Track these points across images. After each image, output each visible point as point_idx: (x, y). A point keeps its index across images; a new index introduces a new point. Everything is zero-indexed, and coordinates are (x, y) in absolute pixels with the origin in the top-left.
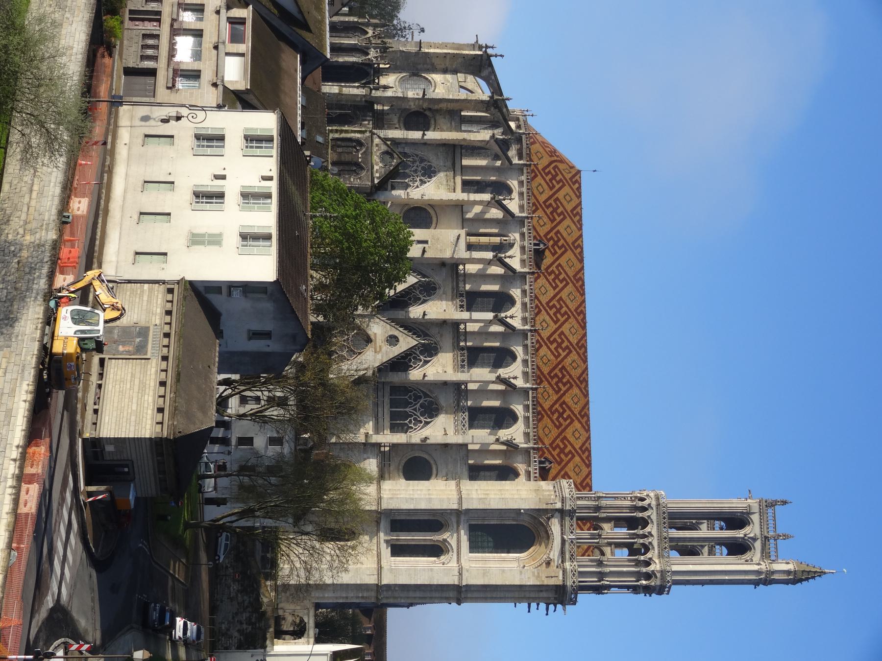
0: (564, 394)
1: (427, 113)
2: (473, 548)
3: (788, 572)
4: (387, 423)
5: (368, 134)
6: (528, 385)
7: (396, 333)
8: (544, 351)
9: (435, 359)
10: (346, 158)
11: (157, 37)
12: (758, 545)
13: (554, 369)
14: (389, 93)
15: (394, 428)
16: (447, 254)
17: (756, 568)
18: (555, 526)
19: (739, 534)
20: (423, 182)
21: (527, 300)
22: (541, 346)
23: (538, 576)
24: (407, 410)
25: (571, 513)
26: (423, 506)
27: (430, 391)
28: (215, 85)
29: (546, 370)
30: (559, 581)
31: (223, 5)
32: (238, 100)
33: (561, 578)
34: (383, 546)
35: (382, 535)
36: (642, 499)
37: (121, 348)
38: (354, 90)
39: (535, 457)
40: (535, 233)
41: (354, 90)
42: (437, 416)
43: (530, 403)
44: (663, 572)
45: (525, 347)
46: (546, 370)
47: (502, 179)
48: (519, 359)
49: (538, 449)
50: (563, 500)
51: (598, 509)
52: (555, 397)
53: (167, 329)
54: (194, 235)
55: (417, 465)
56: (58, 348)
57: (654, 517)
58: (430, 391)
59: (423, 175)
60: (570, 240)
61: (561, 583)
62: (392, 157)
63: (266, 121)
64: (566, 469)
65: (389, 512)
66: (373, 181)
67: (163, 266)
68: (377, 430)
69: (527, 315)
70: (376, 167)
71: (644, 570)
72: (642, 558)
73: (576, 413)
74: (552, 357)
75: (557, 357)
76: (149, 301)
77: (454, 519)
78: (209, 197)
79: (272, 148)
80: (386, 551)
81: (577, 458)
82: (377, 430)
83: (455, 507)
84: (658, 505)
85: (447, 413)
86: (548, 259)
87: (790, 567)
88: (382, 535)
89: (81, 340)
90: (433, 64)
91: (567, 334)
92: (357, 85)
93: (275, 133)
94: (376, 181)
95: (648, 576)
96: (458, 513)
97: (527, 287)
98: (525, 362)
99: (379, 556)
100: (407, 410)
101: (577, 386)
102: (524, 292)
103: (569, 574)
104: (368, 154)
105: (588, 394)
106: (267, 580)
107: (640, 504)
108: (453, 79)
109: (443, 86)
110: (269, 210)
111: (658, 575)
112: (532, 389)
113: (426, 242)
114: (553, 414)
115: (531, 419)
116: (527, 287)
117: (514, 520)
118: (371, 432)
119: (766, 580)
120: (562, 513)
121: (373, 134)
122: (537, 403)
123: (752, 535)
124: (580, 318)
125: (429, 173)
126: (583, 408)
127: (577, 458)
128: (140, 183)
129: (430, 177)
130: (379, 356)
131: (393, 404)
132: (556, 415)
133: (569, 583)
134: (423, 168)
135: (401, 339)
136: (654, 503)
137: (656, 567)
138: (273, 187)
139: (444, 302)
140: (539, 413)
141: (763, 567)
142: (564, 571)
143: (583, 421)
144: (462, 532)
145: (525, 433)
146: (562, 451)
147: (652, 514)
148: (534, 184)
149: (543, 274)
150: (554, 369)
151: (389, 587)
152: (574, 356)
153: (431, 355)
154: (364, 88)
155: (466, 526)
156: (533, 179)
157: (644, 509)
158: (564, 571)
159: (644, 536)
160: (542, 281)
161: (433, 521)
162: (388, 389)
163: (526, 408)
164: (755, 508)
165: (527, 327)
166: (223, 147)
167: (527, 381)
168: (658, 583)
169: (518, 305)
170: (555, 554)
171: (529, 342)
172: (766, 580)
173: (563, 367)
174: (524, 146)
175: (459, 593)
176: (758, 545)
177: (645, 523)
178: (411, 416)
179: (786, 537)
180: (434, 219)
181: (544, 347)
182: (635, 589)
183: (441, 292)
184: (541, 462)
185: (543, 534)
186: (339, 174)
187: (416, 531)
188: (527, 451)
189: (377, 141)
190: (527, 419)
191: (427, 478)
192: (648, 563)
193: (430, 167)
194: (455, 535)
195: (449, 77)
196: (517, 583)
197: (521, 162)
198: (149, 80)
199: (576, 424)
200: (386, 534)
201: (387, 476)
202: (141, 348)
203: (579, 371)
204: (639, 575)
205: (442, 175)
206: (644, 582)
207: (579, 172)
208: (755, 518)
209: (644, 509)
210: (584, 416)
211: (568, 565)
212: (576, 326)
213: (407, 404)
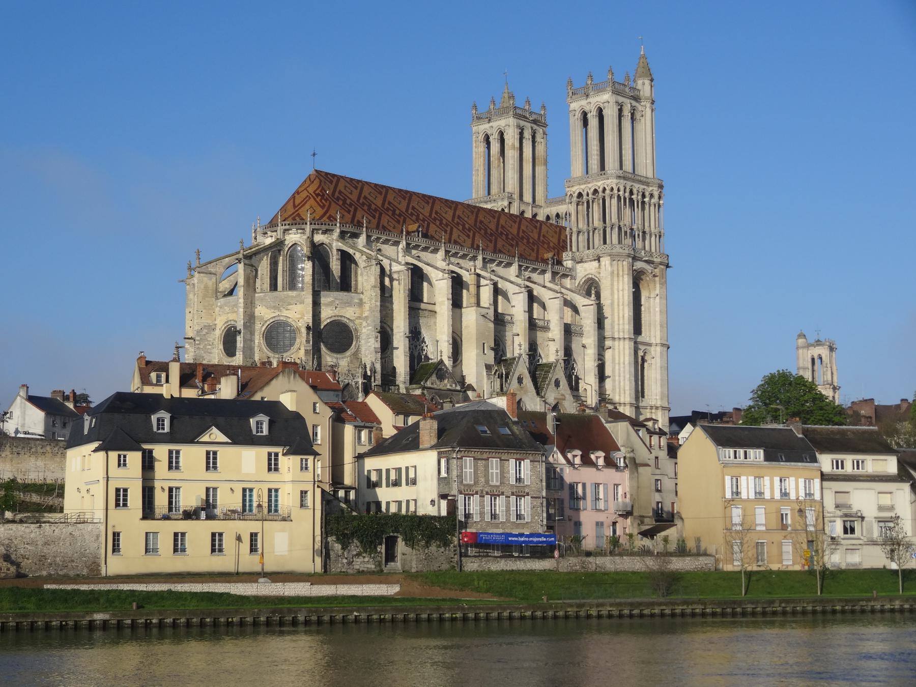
7: (553, 380)
20: (423, 341)
36: (619, 190)
48: (495, 268)
59: (418, 340)
70: (449, 387)
87: (647, 82)
108: (326, 296)
129: (420, 333)
130: (567, 396)
136: (622, 181)
139: (507, 333)
141: (648, 105)
145: (539, 274)
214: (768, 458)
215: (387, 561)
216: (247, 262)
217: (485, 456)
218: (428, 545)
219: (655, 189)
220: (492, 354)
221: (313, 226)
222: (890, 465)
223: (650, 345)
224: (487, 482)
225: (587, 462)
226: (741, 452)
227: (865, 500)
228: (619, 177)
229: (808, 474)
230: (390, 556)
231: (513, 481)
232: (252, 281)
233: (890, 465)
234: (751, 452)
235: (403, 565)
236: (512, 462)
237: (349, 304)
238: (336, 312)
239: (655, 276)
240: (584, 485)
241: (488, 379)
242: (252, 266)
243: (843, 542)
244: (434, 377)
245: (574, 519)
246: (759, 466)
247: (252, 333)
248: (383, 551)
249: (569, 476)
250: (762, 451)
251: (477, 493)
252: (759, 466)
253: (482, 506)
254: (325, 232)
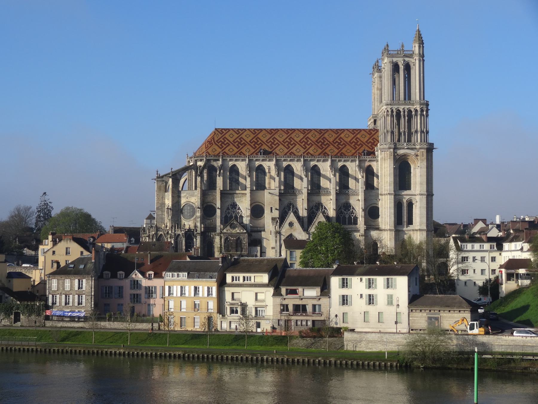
0: (329, 141)
1: (204, 206)
2: (409, 189)
3: (419, 47)
4: (354, 226)
5: (222, 235)
8: (310, 151)
9: (324, 204)
10: (234, 245)
11: (297, 321)
12: (407, 59)
13: (318, 146)
14: (198, 224)
15: (356, 223)
16: (277, 198)
17: (417, 62)
18: (401, 152)
19: (402, 68)
20: (239, 209)
21: (289, 159)
22: (309, 153)
23: (422, 160)
24: (347, 217)
25: (395, 145)
26: (393, 211)
28: (319, 299)
29: (320, 151)
30: (425, 151)
31: (281, 297)
32: (325, 290)
34: (409, 228)
35: (404, 229)
37: (437, 325)
38: (198, 242)
39: (363, 158)
40: (254, 154)
41: (198, 242)
42: (350, 204)
43: (337, 159)
44: (421, 104)
45: (311, 160)
46: (320, 151)
47: (228, 169)
48: (317, 164)
49: (359, 156)
50: (390, 148)
51: (392, 133)
53: (428, 311)
54: (388, 304)
55: (372, 213)
56: (483, 333)
57: (396, 107)
59: (236, 208)
60: (253, 136)
62: (233, 223)
63: (335, 281)
64: (364, 142)
65: (395, 227)
66: (245, 233)
67: (402, 313)
68: (358, 231)
69: (296, 159)
70: (238, 231)
71: (419, 113)
72: (413, 113)
73: (336, 136)
74: (313, 147)
75: (312, 145)
76: (417, 317)
77: (397, 197)
78: (371, 300)
79: (347, 279)
80: (411, 227)
81: (358, 136)
82: (358, 231)
83: (393, 196)
84: (391, 105)
85: (349, 199)
86: (264, 147)
87: (417, 45)
88: (404, 229)
89: (480, 327)
90: (176, 202)
92: (195, 240)
93: (341, 277)
94: (245, 231)
95: (422, 111)
96: (395, 195)
97: (283, 159)
98: (318, 161)
99: (413, 230)
100: (347, 217)
101: (323, 134)
102: (284, 160)
103: (422, 146)
104: (232, 235)
105: (327, 129)
106: (425, 280)
107: (390, 113)
108: (184, 193)
109: (192, 198)
110: (376, 279)
111: (422, 106)
112: (331, 158)
113: (271, 208)
114: (340, 148)
116: (283, 159)
118: (359, 234)
119: (422, 56)
120: (395, 149)
121: (221, 233)
122: (336, 156)
123: (402, 62)
124: (291, 132)
125: (234, 206)
126: (334, 132)
127: (358, 136)
128: (365, 323)
129: (236, 205)
132: (340, 146)
133: (426, 147)
134: (232, 208)
135: (319, 220)
136: (390, 107)
137: (418, 107)
138: (365, 278)
140: (341, 155)
141: (417, 58)
142: (420, 148)
143: (340, 132)
144: (403, 193)
147: (395, 108)
148: (230, 154)
149: (273, 150)
150: (318, 146)
151: (427, 226)
152: (309, 136)
153: (322, 206)
154: (196, 237)
155: (400, 191)
156: (227, 154)
157: (392, 111)
158: (420, 148)
159: (404, 112)
160: (277, 151)
161: (398, 206)
163: (340, 161)
164: (390, 59)
165: (302, 160)
166: (347, 296)
167: (327, 160)
168: (425, 106)
169: (291, 163)
170: (412, 152)
171: (309, 159)
172: (422, 56)
173: (316, 141)
174: (212, 158)
175: (429, 195)
176: (407, 59)
177: (398, 112)
179: (403, 46)
180: (257, 203)
181: (309, 151)
182: (427, 116)
184: (364, 155)
185: (403, 157)
186: (242, 249)
187: (402, 214)
188: (360, 161)
189: (225, 231)
190: (345, 161)
191: (377, 209)
192: (416, 111)
193: (231, 205)
194: (405, 197)
195: (182, 195)
196: (425, 170)
197: (221, 160)
198: (316, 323)
199: (342, 136)
200: (404, 227)
201: (377, 227)
202: (437, 319)
203: (316, 133)
204: (422, 115)
205: (235, 200)
206: (425, 113)
207: (216, 129)
208: (395, 60)
209: (392, 111)
210: (338, 132)
211: (418, 147)
213: (344, 218)
214: (189, 277)
215: (15, 322)
216: (159, 179)
217: (63, 278)
218: (30, 316)
219: (418, 106)
220: (277, 212)
221: (195, 159)
222: (264, 278)
223: (415, 195)
224: (64, 289)
225: (158, 275)
226: (176, 274)
227: (246, 296)
228: (387, 105)
229: (209, 285)
230: (17, 319)
231: (76, 288)
232: (163, 188)
233: (264, 278)
234: (181, 274)
235: (22, 323)
236: (77, 281)
237: (193, 195)
238: (187, 200)
239: (417, 156)
240: (155, 287)
241: (273, 225)
242: (163, 181)
243: (228, 318)
244: (228, 227)
245: (148, 303)
246: (183, 281)
247: (163, 211)
248: (13, 318)
249: (145, 283)
250: (186, 273)
251: (58, 294)
252: (183, 281)
253: (60, 299)
254: (201, 160)
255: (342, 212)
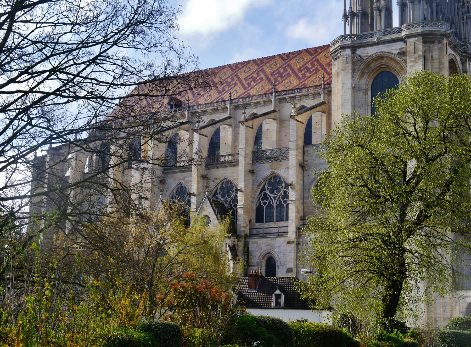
6: (273, 100)
24: (275, 205)
27: (259, 186)
33: (416, 39)
52: (293, 77)
58: (259, 186)
61: (421, 38)
74: (260, 84)
91: (248, 74)
100: (275, 205)
115: (301, 94)
117: (366, 93)
131: (270, 220)
146: (315, 58)
153: (232, 186)
158: (409, 36)
162: (258, 225)
170: (395, 48)
178: (280, 201)
183: (183, 182)
212: (245, 68)
213: (270, 206)
255: (265, 197)
